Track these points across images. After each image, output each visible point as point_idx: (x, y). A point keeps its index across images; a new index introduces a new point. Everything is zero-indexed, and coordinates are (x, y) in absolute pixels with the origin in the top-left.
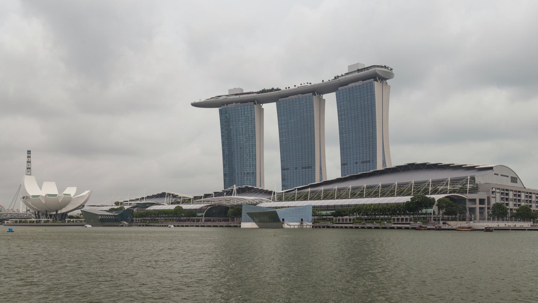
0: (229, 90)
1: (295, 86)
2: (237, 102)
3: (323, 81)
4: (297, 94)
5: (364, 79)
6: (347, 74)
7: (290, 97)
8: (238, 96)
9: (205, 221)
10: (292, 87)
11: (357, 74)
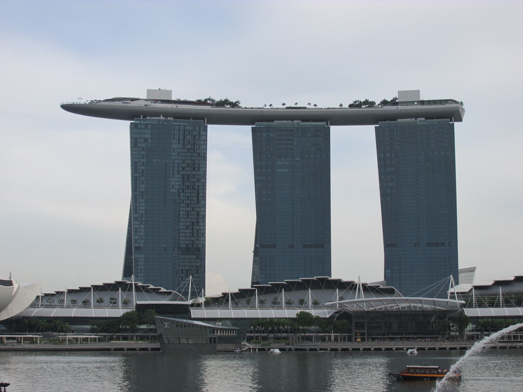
0: (149, 91)
1: (284, 104)
2: (166, 114)
3: (341, 105)
4: (292, 120)
5: (429, 116)
6: (394, 102)
7: (276, 122)
8: (174, 106)
9: (336, 339)
10: (277, 105)
11: (420, 107)
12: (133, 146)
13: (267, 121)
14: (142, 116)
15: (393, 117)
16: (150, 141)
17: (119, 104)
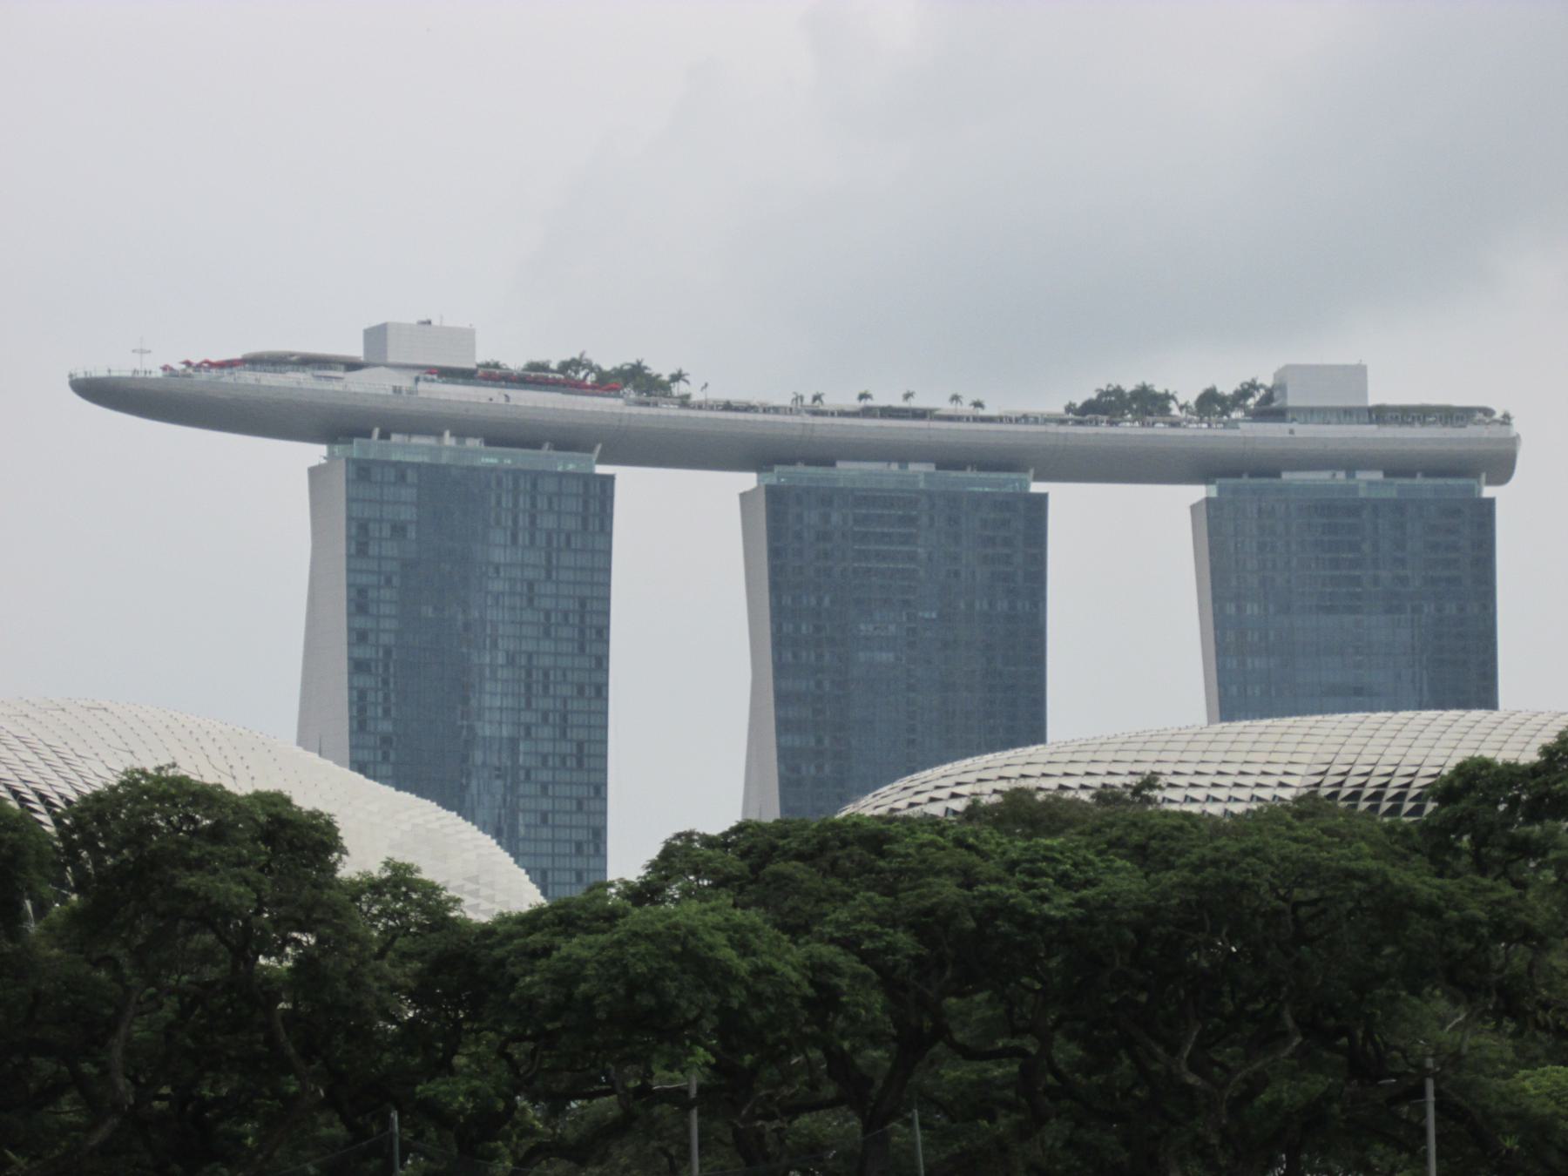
1: (863, 396)
4: (903, 460)
12: (353, 551)
13: (810, 462)
14: (376, 431)
15: (1265, 467)
16: (412, 533)
17: (301, 380)
